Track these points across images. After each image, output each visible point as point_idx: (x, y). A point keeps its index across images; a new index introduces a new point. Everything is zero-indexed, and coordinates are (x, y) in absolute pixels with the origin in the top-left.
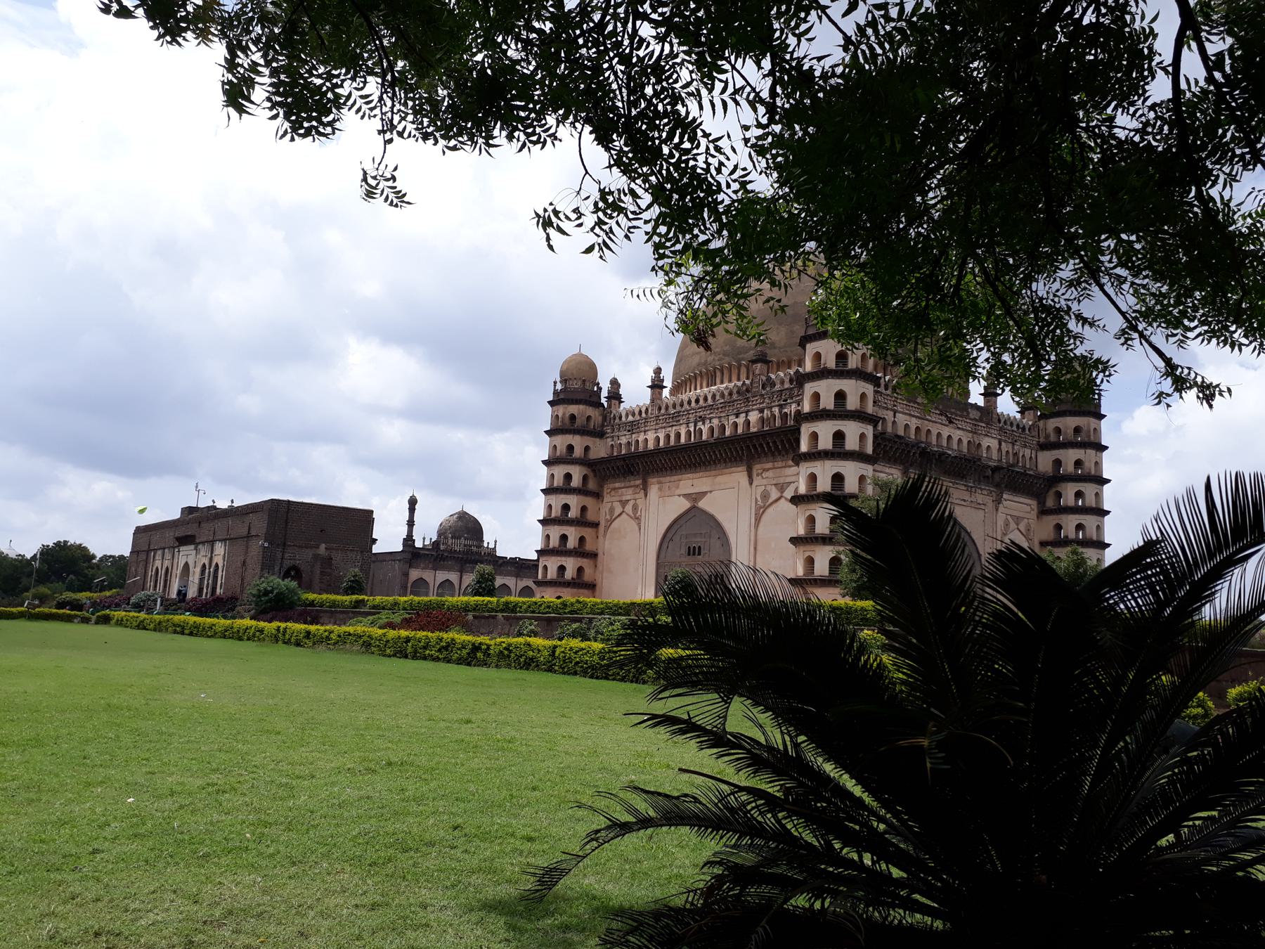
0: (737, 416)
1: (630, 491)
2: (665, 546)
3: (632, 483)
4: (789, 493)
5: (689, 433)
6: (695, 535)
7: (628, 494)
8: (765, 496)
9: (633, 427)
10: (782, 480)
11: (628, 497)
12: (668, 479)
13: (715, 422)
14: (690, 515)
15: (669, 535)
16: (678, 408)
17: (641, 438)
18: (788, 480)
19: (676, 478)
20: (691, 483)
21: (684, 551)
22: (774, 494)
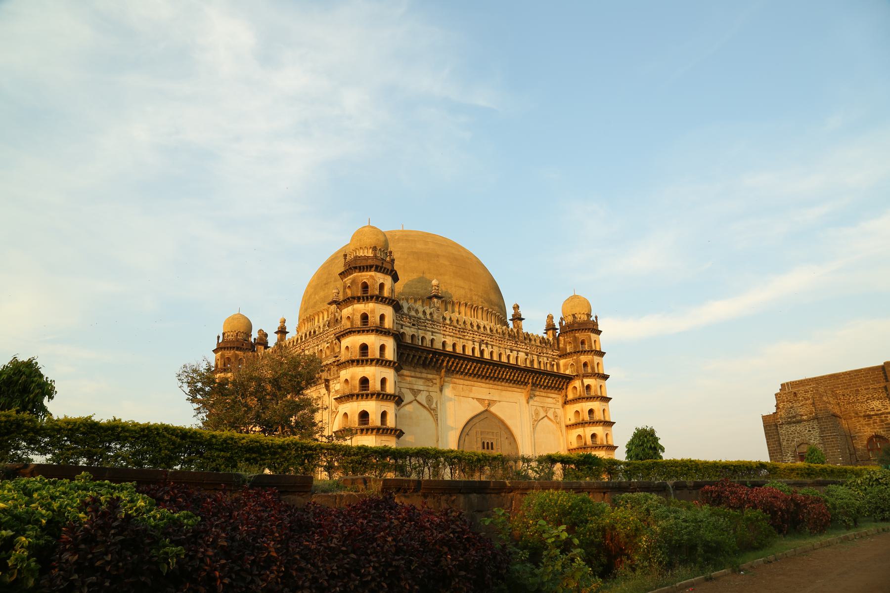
0: (512, 351)
1: (421, 382)
2: (462, 439)
3: (424, 375)
5: (473, 349)
6: (488, 433)
10: (546, 405)
11: (421, 388)
12: (461, 382)
13: (496, 350)
14: (482, 417)
15: (467, 430)
17: (429, 337)
18: (549, 406)
19: (469, 382)
20: (483, 390)
21: (480, 445)
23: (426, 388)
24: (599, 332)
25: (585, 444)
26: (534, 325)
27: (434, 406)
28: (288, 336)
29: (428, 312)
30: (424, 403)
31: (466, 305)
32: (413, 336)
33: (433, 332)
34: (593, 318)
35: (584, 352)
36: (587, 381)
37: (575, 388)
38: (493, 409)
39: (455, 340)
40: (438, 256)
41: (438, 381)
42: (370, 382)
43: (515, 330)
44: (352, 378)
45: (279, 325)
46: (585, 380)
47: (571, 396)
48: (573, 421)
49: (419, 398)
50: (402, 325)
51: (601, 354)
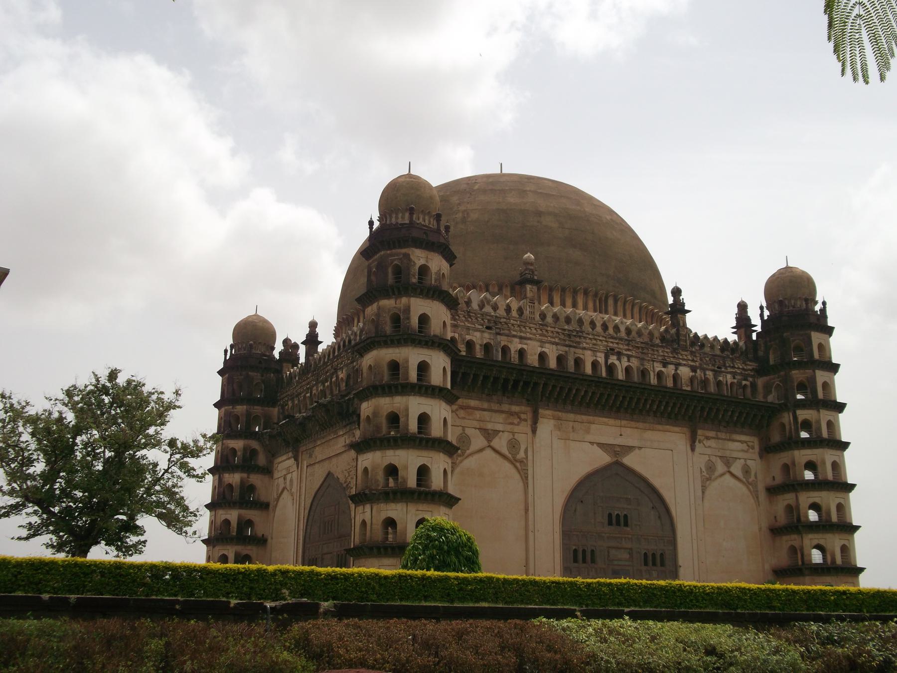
0: (665, 365)
1: (500, 418)
3: (505, 407)
4: (736, 469)
5: (595, 364)
7: (496, 422)
8: (711, 468)
9: (493, 325)
10: (727, 454)
11: (499, 427)
12: (571, 416)
16: (574, 326)
17: (515, 346)
18: (735, 455)
19: (585, 418)
20: (608, 430)
22: (720, 468)
23: (509, 427)
24: (829, 331)
25: (799, 520)
26: (711, 319)
27: (521, 455)
28: (320, 348)
29: (515, 306)
30: (505, 451)
31: (586, 293)
32: (487, 347)
33: (521, 338)
34: (818, 308)
35: (800, 365)
36: (803, 414)
37: (783, 425)
38: (628, 460)
39: (562, 349)
40: (539, 214)
41: (529, 416)
42: (402, 420)
43: (673, 331)
44: (376, 414)
45: (307, 330)
46: (799, 412)
47: (776, 438)
48: (779, 479)
49: (495, 443)
50: (468, 329)
51: (835, 368)
